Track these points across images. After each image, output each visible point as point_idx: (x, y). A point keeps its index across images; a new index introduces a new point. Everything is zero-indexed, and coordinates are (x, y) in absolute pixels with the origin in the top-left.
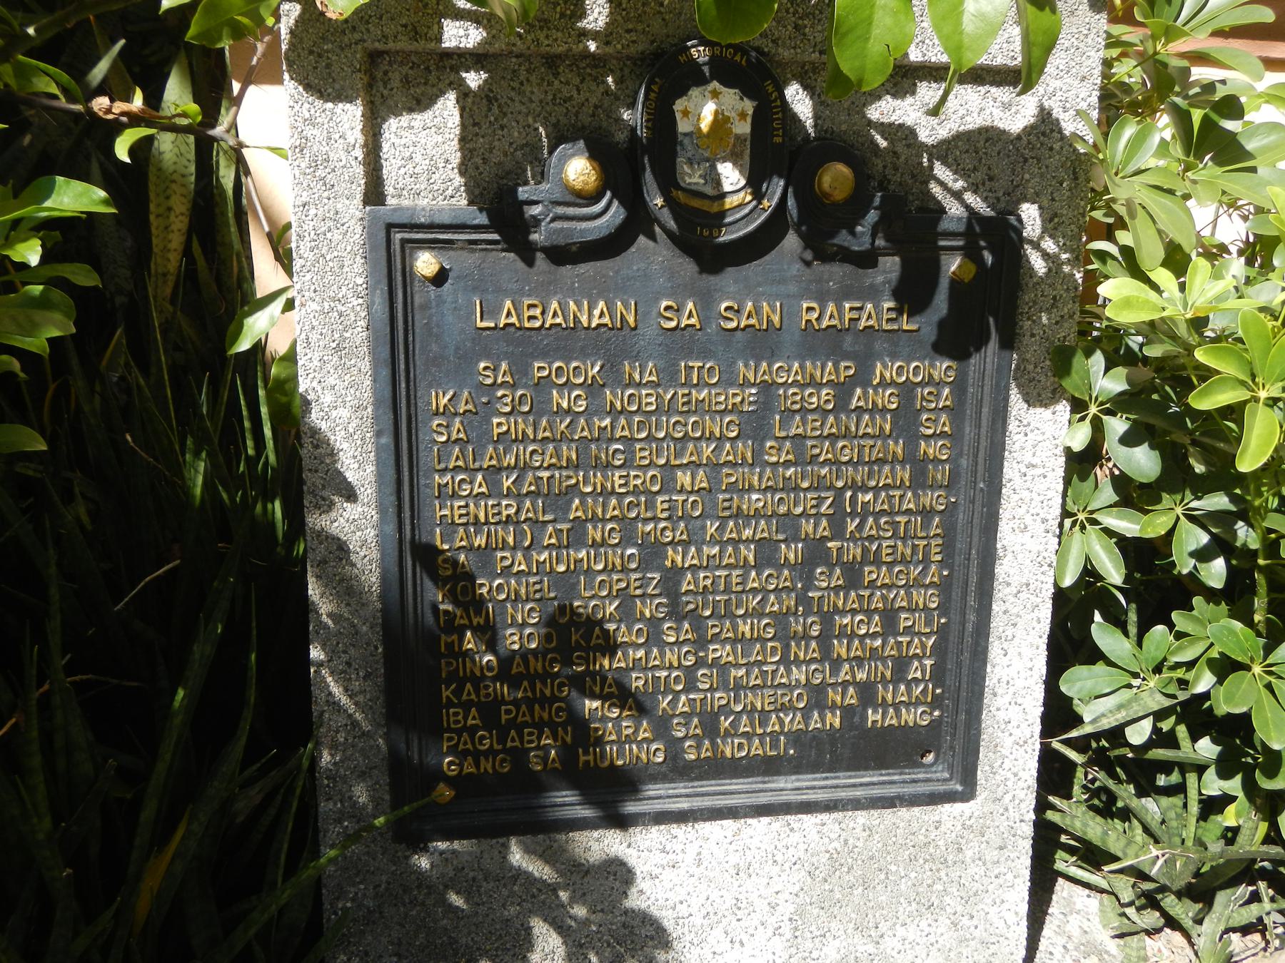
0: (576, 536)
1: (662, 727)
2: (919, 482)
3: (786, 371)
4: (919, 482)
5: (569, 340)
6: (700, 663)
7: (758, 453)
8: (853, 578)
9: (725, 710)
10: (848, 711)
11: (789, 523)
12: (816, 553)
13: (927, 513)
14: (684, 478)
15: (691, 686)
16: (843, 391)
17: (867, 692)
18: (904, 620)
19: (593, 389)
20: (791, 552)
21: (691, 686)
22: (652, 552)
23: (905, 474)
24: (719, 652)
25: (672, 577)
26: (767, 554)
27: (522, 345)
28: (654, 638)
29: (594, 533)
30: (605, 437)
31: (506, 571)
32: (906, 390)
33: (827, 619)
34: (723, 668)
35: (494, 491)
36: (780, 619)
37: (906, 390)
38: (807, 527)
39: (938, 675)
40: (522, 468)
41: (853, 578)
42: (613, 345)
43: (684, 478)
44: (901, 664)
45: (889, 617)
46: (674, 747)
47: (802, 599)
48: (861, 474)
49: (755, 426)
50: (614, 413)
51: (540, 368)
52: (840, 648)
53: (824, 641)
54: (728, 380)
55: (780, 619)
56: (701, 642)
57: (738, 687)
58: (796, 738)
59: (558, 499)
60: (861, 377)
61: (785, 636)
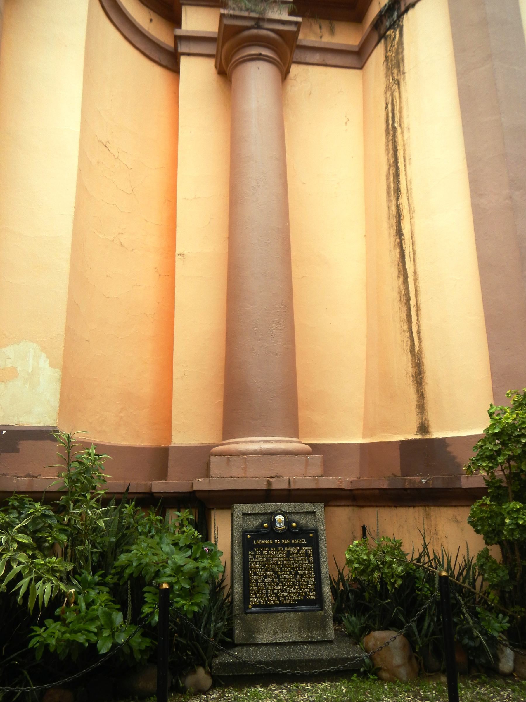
0: (266, 571)
1: (279, 599)
2: (309, 563)
3: (290, 549)
4: (309, 563)
5: (265, 545)
6: (283, 589)
7: (288, 559)
8: (302, 576)
9: (287, 596)
10: (303, 596)
11: (293, 569)
12: (297, 573)
13: (311, 567)
14: (279, 562)
15: (282, 592)
16: (298, 551)
17: (306, 593)
18: (310, 583)
19: (268, 551)
20: (294, 573)
21: (282, 592)
22: (276, 573)
23: (307, 562)
24: (285, 587)
25: (279, 576)
26: (291, 573)
27: (259, 546)
28: (277, 585)
29: (268, 570)
30: (269, 557)
31: (258, 575)
32: (306, 551)
33: (299, 582)
34: (286, 589)
35: (256, 564)
36: (293, 582)
37: (306, 551)
38: (295, 569)
39: (315, 591)
40: (260, 561)
41: (302, 576)
42: (270, 546)
43: (279, 562)
44: (310, 589)
45: (308, 582)
46: (280, 601)
47: (296, 580)
48: (301, 562)
49: (287, 556)
50: (270, 554)
51: (261, 549)
52: (301, 587)
53: (299, 585)
54: (284, 550)
55: (293, 582)
56: (283, 586)
57: (288, 592)
58: (297, 600)
59: (264, 566)
60: (300, 549)
61: (294, 585)
